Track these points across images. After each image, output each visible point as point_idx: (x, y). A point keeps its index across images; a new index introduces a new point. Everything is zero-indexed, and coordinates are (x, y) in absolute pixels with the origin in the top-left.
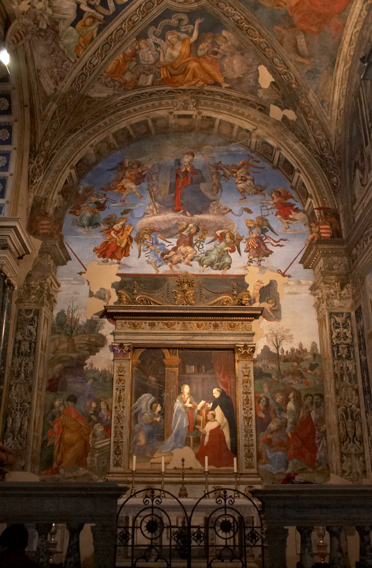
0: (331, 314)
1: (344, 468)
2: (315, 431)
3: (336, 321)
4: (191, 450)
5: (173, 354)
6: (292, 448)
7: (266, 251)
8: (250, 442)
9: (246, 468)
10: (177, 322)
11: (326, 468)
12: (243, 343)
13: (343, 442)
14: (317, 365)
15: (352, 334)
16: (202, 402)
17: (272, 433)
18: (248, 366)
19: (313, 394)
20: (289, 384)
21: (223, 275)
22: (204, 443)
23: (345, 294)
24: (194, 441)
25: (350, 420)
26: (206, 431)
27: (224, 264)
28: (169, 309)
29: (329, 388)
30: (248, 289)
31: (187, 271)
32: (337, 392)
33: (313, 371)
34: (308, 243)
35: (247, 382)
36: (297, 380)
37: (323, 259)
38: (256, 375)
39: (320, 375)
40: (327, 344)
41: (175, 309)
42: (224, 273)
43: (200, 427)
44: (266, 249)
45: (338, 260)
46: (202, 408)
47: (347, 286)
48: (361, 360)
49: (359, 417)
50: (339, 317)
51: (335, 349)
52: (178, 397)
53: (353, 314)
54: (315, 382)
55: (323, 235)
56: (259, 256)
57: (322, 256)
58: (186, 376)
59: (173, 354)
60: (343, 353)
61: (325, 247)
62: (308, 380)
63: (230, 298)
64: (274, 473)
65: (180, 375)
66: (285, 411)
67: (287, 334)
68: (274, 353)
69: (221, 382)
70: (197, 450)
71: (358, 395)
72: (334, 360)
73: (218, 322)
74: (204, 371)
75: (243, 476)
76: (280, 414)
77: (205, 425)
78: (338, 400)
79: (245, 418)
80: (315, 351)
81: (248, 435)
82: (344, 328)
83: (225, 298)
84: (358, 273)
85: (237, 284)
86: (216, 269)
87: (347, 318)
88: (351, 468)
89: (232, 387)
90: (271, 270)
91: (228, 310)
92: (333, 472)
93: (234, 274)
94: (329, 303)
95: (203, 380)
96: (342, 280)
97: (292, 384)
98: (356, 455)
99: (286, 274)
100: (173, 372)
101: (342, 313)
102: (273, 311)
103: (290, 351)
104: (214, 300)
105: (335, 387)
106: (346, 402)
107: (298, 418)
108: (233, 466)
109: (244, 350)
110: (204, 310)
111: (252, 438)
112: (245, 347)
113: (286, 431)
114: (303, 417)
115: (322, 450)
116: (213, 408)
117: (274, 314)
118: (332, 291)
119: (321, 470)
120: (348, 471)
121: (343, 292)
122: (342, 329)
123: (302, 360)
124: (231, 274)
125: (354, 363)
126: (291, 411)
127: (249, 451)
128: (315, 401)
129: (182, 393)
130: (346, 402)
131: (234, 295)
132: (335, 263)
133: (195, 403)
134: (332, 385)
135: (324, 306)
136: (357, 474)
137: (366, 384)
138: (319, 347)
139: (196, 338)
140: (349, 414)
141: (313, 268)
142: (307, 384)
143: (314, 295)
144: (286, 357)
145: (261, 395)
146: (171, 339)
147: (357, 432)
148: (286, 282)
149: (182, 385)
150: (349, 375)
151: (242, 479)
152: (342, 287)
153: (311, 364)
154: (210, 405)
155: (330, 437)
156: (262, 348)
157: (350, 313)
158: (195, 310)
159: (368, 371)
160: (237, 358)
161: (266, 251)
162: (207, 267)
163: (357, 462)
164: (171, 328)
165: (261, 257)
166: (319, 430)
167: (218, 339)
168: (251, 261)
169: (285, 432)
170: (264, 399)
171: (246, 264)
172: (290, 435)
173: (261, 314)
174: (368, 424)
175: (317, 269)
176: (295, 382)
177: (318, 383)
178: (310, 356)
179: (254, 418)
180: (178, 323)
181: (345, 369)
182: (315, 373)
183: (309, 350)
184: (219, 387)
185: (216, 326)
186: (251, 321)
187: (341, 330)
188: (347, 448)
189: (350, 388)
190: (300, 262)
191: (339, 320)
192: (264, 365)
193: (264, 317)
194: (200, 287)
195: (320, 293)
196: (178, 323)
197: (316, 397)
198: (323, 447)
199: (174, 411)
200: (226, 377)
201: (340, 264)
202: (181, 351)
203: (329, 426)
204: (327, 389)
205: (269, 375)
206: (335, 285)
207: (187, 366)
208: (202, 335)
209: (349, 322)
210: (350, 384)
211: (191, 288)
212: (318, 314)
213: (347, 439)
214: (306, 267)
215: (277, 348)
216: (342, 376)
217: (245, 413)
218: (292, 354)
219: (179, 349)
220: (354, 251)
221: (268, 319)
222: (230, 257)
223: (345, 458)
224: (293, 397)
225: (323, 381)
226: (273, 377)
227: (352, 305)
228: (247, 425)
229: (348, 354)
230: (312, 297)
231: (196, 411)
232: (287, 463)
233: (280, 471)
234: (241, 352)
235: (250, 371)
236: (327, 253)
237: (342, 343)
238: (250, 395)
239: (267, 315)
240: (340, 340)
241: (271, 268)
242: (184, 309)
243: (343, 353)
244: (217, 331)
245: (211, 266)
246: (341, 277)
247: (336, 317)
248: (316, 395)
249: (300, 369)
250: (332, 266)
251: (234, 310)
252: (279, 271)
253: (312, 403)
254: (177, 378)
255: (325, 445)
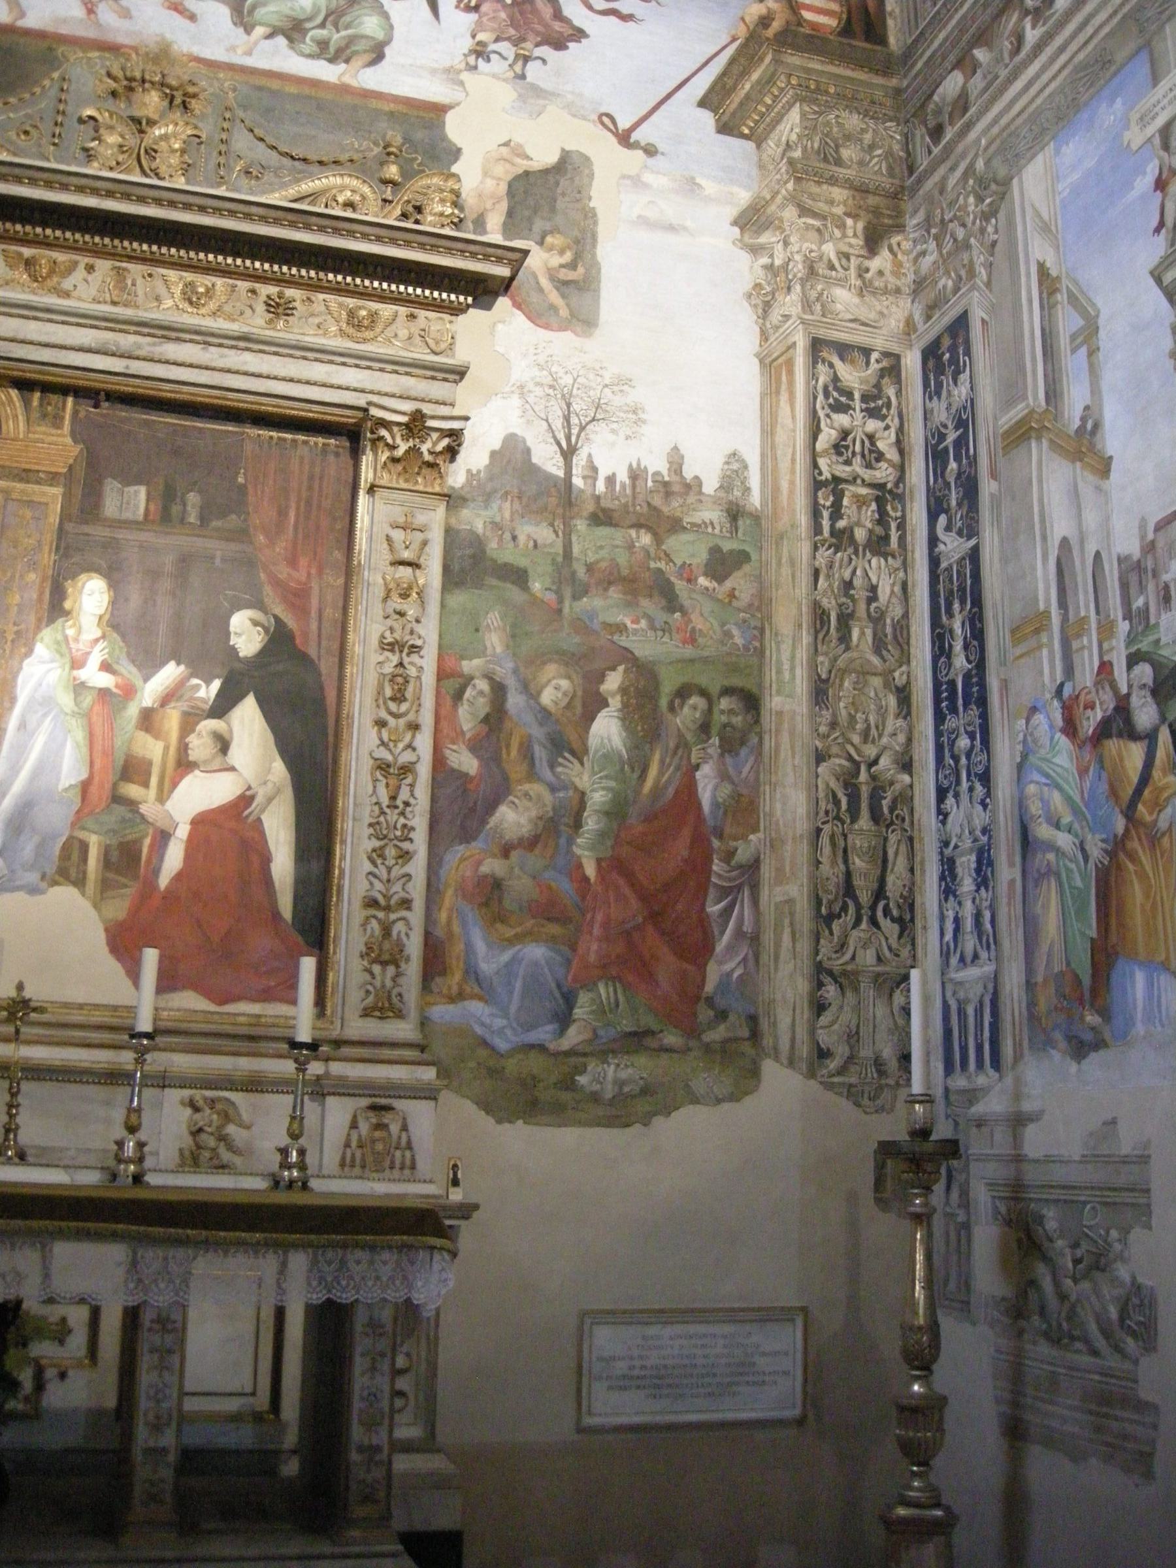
0: (817, 346)
1: (824, 1038)
2: (708, 861)
3: (836, 379)
4: (85, 905)
5: (44, 416)
6: (596, 931)
7: (557, 26)
8: (397, 887)
9: (366, 1013)
10: (83, 260)
11: (745, 1033)
12: (408, 407)
13: (830, 918)
14: (742, 558)
15: (899, 444)
16: (170, 672)
17: (506, 851)
18: (420, 519)
19: (715, 690)
20: (607, 626)
21: (344, 89)
22: (157, 872)
23: (881, 273)
24: (107, 863)
25: (864, 822)
26: (177, 818)
27: (351, 40)
28: (49, 185)
29: (786, 666)
30: (455, 169)
31: (168, 36)
32: (820, 692)
33: (720, 578)
34: (742, 32)
35: (405, 596)
36: (646, 616)
37: (803, 115)
38: (456, 567)
39: (751, 605)
40: (793, 472)
41: (81, 189)
42: (348, 80)
43: (144, 796)
44: (558, 15)
45: (863, 131)
46: (167, 699)
47: (894, 240)
48: (934, 561)
49: (905, 812)
50: (852, 362)
51: (826, 500)
52: (47, 634)
53: (912, 362)
54: (728, 634)
55: (807, 15)
56: (522, 39)
57: (803, 100)
58: (98, 532)
59: (44, 416)
60: (858, 524)
61: (811, 65)
62: (698, 622)
63: (366, 190)
64: (502, 1045)
65: (69, 527)
66: (579, 753)
67: (618, 401)
68: (549, 477)
69: (276, 583)
70: (118, 908)
71: (909, 713)
72: (816, 548)
73: (290, 292)
74: (192, 518)
75: (346, 1051)
76: (552, 766)
77: (175, 785)
78: (823, 729)
79: (383, 767)
80: (737, 493)
81: (390, 852)
82: (873, 413)
83: (342, 189)
84: (970, 171)
85: (406, 140)
86: (310, 56)
87: (882, 373)
88: (853, 1037)
89: (328, 612)
90: (575, 112)
91: (351, 234)
92: (777, 1059)
93: (395, 92)
94: (813, 294)
95: (185, 561)
96: (876, 212)
97: (621, 629)
98: (878, 980)
99: (634, 137)
100: (30, 504)
101: (866, 352)
102: (563, 285)
103: (623, 477)
104: (284, 186)
105: (813, 666)
106: (856, 739)
107: (637, 792)
108: (294, 1002)
109: (405, 438)
110: (232, 213)
111: (407, 869)
112: (416, 425)
113: (578, 851)
114: (657, 791)
115: (731, 949)
116: (222, 707)
117: (563, 296)
118: (829, 249)
119: (725, 1041)
120: (841, 1051)
121: (875, 264)
122: (858, 415)
123: (676, 526)
124: (384, 89)
125: (901, 574)
126: (605, 756)
127: (387, 931)
128: (719, 719)
129: (67, 614)
130: (856, 739)
131: (386, 182)
132: (848, 137)
133: (130, 671)
134: (802, 654)
135: (790, 303)
136: (878, 1063)
137: (960, 662)
138: (755, 482)
139: (172, 350)
140: (865, 792)
141: (758, 139)
142: (692, 640)
143: (755, 250)
144: (604, 503)
145: (468, 666)
146: (44, 339)
147: (890, 879)
148: (633, 173)
149: (74, 576)
150: (877, 620)
151: (336, 1068)
152: (873, 241)
153: (715, 551)
154: (209, 691)
155: (772, 894)
156: (497, 445)
157: (898, 357)
158: (187, 207)
159: (978, 602)
160: (367, 474)
161: (557, 26)
162: (269, 36)
163: (881, 1011)
164: (50, 283)
165: (528, 45)
166: (731, 854)
167: (282, 373)
168: (480, 52)
169: (569, 852)
170: (483, 685)
171: (458, 62)
172: (590, 870)
173: (506, 286)
174: (946, 844)
175: (772, 146)
176: (636, 621)
177: (739, 641)
178: (712, 515)
179: (424, 770)
180: (90, 268)
181: (861, 594)
182: (732, 595)
183: (710, 486)
184: (260, 605)
185: (278, 309)
186: (456, 310)
187: (854, 420)
188: (842, 946)
189: (876, 682)
190: (703, 103)
191: (852, 376)
192: (496, 526)
193: (517, 305)
194: (226, 116)
195: (780, 246)
196: (90, 268)
197: (725, 703)
198: (739, 933)
199: (13, 700)
200: (303, 562)
201: (872, 147)
202: (86, 409)
203: (774, 844)
204: (779, 672)
205: (519, 577)
206: (842, 226)
207: (111, 488)
208: (205, 337)
209: (891, 392)
210: (875, 660)
211: (177, 115)
212: (764, 336)
213: (844, 908)
214: (725, 128)
215: (568, 454)
216: (845, 620)
217: (383, 744)
218: (634, 497)
219: (79, 392)
220: (953, 83)
221: (534, 317)
222: (386, 16)
223: (830, 991)
224: (623, 690)
225: (762, 630)
226: (536, 586)
227: (910, 324)
228: (385, 801)
229: (879, 530)
230: (745, 257)
231: (132, 711)
232: (569, 1000)
233: (536, 1036)
234: (393, 447)
235: (425, 543)
236: (818, 90)
237: (854, 480)
238: (415, 658)
239: (534, 298)
240: (848, 462)
241: (569, 97)
242: (127, 197)
243: (858, 524)
244: (281, 331)
245: (290, 40)
246: (872, 200)
247: (836, 360)
248: (727, 691)
249: (661, 565)
250: (837, 146)
251: (379, 239)
252: (606, 120)
253: (705, 728)
254: (50, 537)
255: (748, 927)
